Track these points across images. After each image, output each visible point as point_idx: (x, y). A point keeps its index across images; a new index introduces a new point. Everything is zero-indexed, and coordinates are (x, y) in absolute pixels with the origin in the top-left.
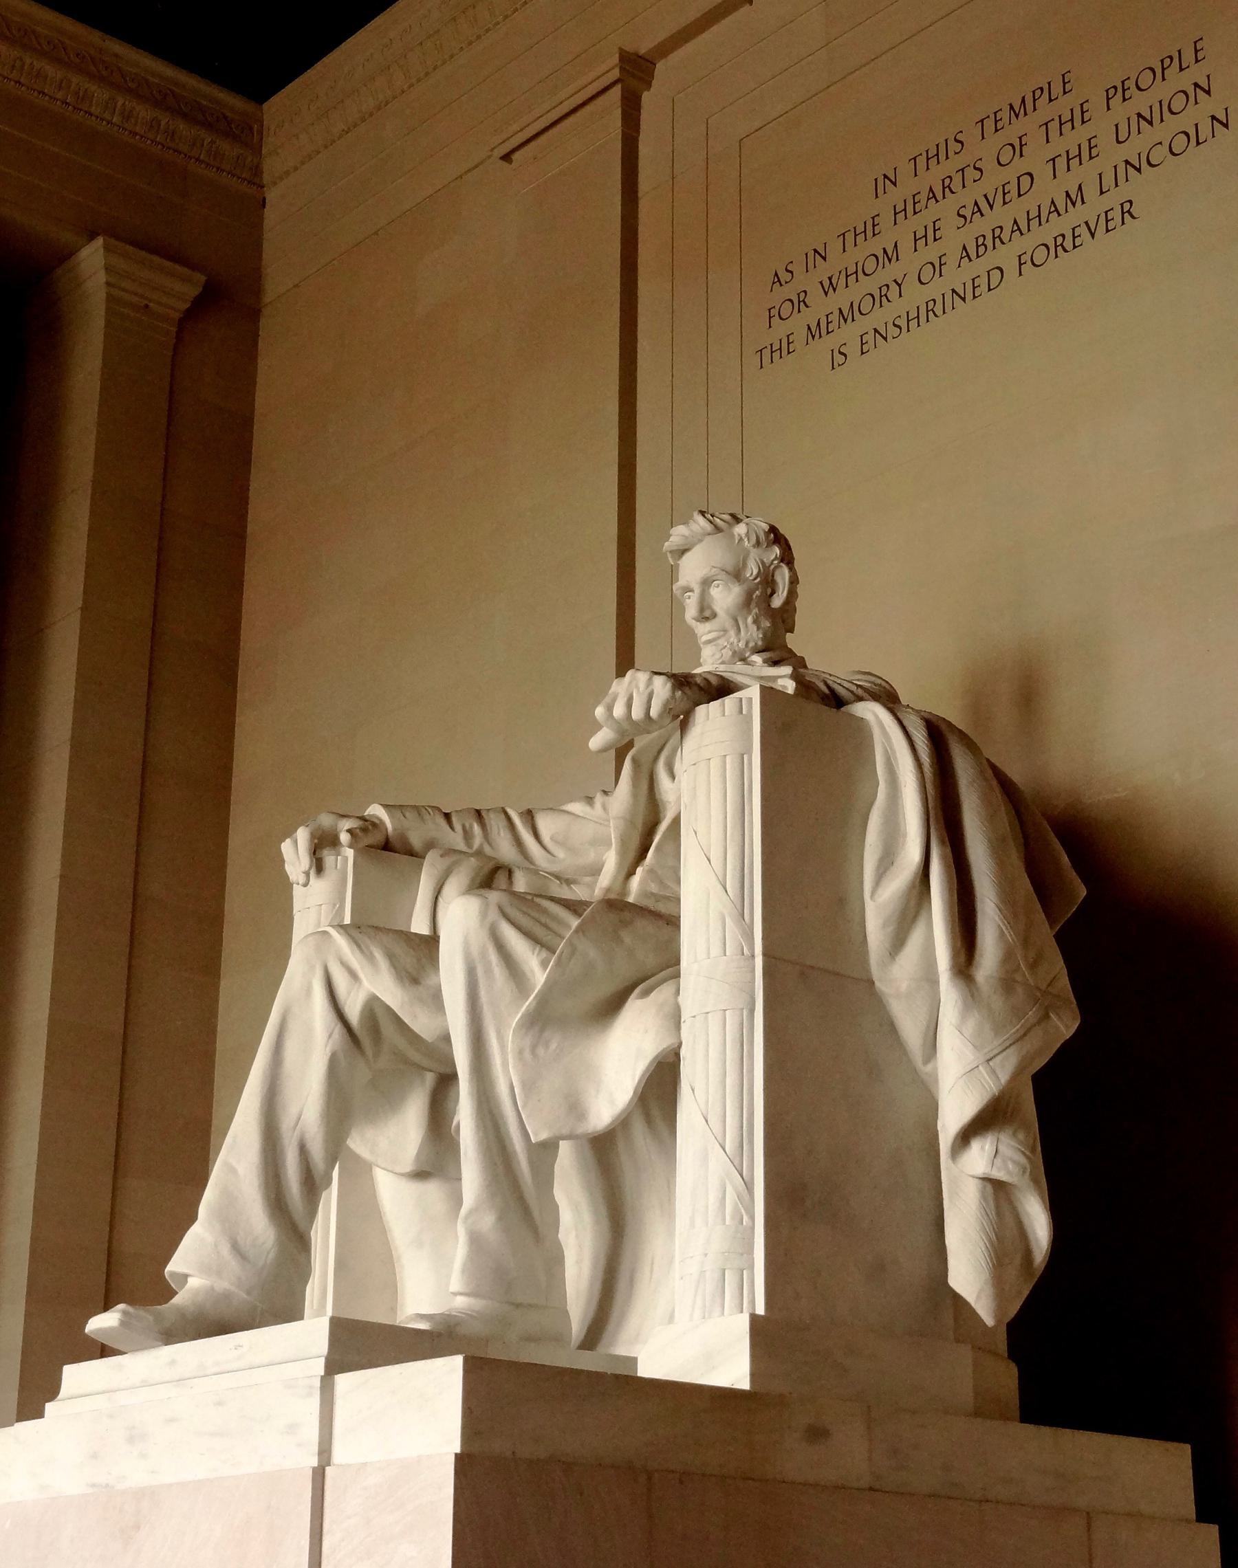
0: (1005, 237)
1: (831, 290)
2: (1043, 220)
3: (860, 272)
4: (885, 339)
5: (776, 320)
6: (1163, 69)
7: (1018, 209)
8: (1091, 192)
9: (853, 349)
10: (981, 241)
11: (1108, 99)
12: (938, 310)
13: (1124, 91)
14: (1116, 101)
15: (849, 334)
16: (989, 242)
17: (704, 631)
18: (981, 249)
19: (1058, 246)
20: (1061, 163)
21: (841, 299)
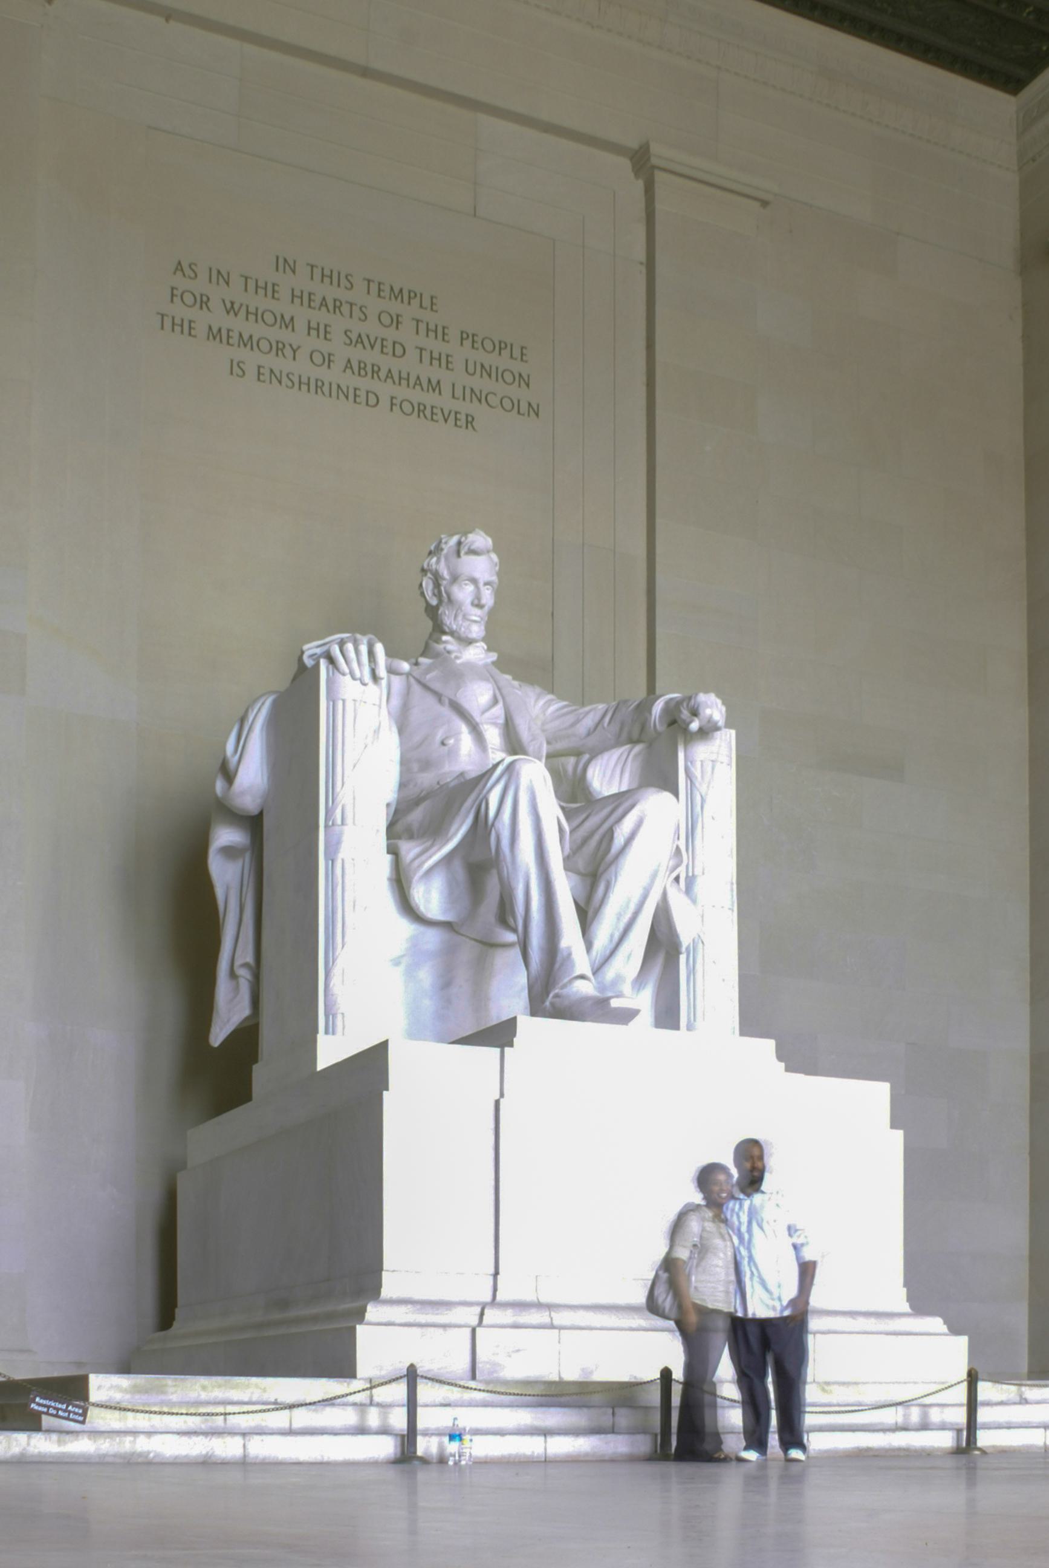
0: (383, 374)
1: (232, 312)
2: (411, 385)
3: (258, 316)
4: (280, 382)
5: (177, 300)
6: (500, 348)
7: (396, 365)
8: (446, 389)
9: (251, 372)
10: (362, 365)
11: (462, 339)
12: (326, 389)
13: (473, 341)
14: (468, 343)
15: (251, 359)
16: (369, 369)
17: (475, 614)
18: (363, 372)
19: (421, 409)
20: (426, 356)
21: (239, 324)
